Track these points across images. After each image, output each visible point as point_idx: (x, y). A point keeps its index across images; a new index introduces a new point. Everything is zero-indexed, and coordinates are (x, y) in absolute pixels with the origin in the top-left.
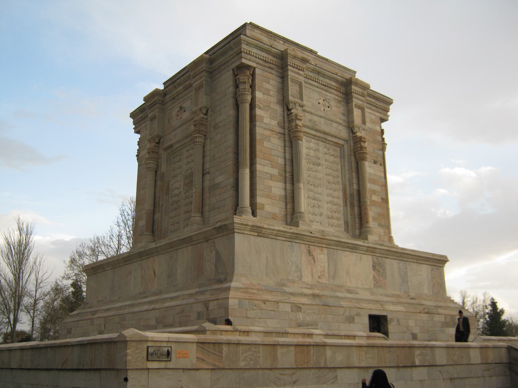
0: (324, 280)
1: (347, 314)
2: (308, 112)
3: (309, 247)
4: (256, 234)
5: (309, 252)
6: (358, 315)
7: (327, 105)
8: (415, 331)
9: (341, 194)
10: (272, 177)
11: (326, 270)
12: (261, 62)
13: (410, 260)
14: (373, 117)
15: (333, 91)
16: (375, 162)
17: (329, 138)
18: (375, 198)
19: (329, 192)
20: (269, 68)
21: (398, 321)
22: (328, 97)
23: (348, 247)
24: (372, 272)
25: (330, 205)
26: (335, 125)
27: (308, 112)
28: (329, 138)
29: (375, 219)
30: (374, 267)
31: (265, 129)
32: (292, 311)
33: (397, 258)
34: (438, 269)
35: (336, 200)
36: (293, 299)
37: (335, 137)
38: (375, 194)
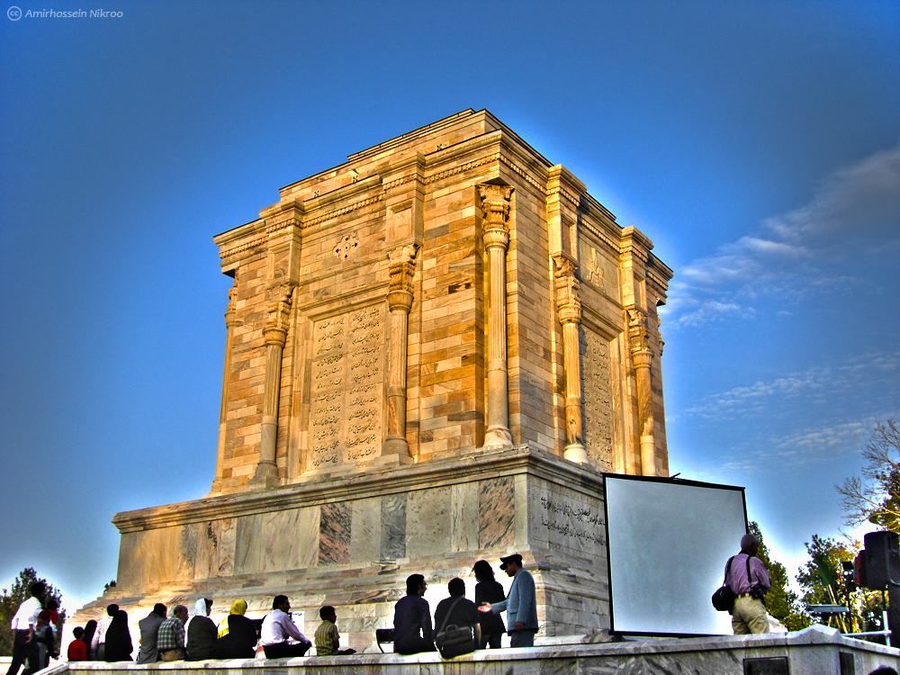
0: (228, 572)
2: (314, 280)
3: (210, 524)
4: (142, 528)
7: (352, 241)
11: (233, 554)
12: (247, 253)
13: (412, 488)
14: (458, 197)
15: (368, 209)
16: (452, 290)
17: (358, 299)
18: (443, 366)
20: (257, 253)
22: (355, 228)
23: (269, 505)
24: (318, 536)
26: (362, 271)
27: (314, 280)
28: (358, 299)
30: (323, 526)
31: (244, 351)
33: (377, 493)
34: (504, 484)
35: (369, 406)
37: (366, 291)
38: (444, 358)
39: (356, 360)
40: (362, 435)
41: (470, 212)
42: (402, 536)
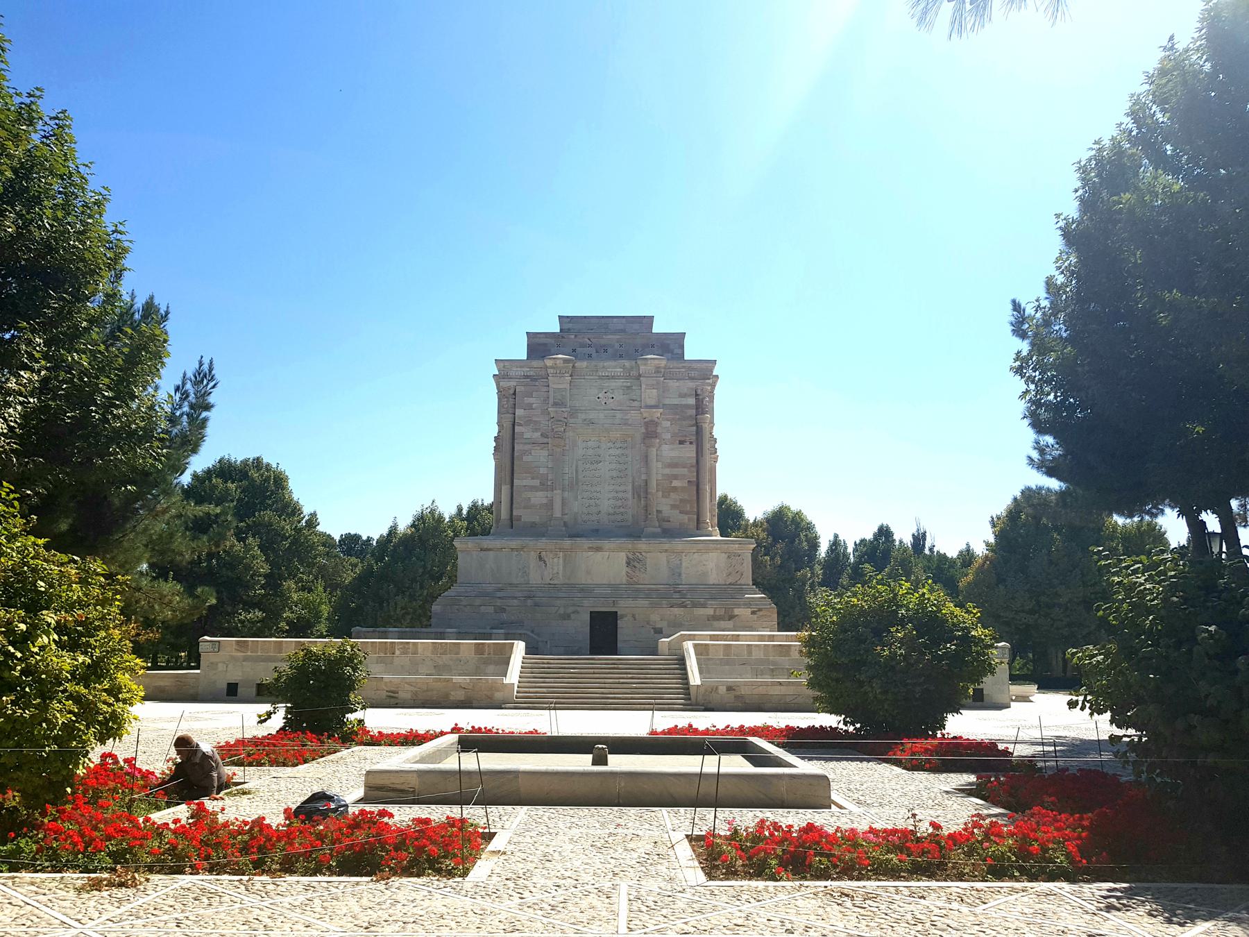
1: (562, 611)
5: (540, 558)
6: (576, 612)
8: (658, 626)
9: (630, 487)
10: (533, 488)
16: (681, 442)
18: (676, 483)
19: (611, 488)
21: (634, 616)
25: (612, 502)
29: (673, 507)
30: (628, 564)
32: (496, 612)
35: (620, 495)
36: (499, 602)
39: (613, 466)
40: (617, 511)
41: (692, 401)
42: (680, 575)
